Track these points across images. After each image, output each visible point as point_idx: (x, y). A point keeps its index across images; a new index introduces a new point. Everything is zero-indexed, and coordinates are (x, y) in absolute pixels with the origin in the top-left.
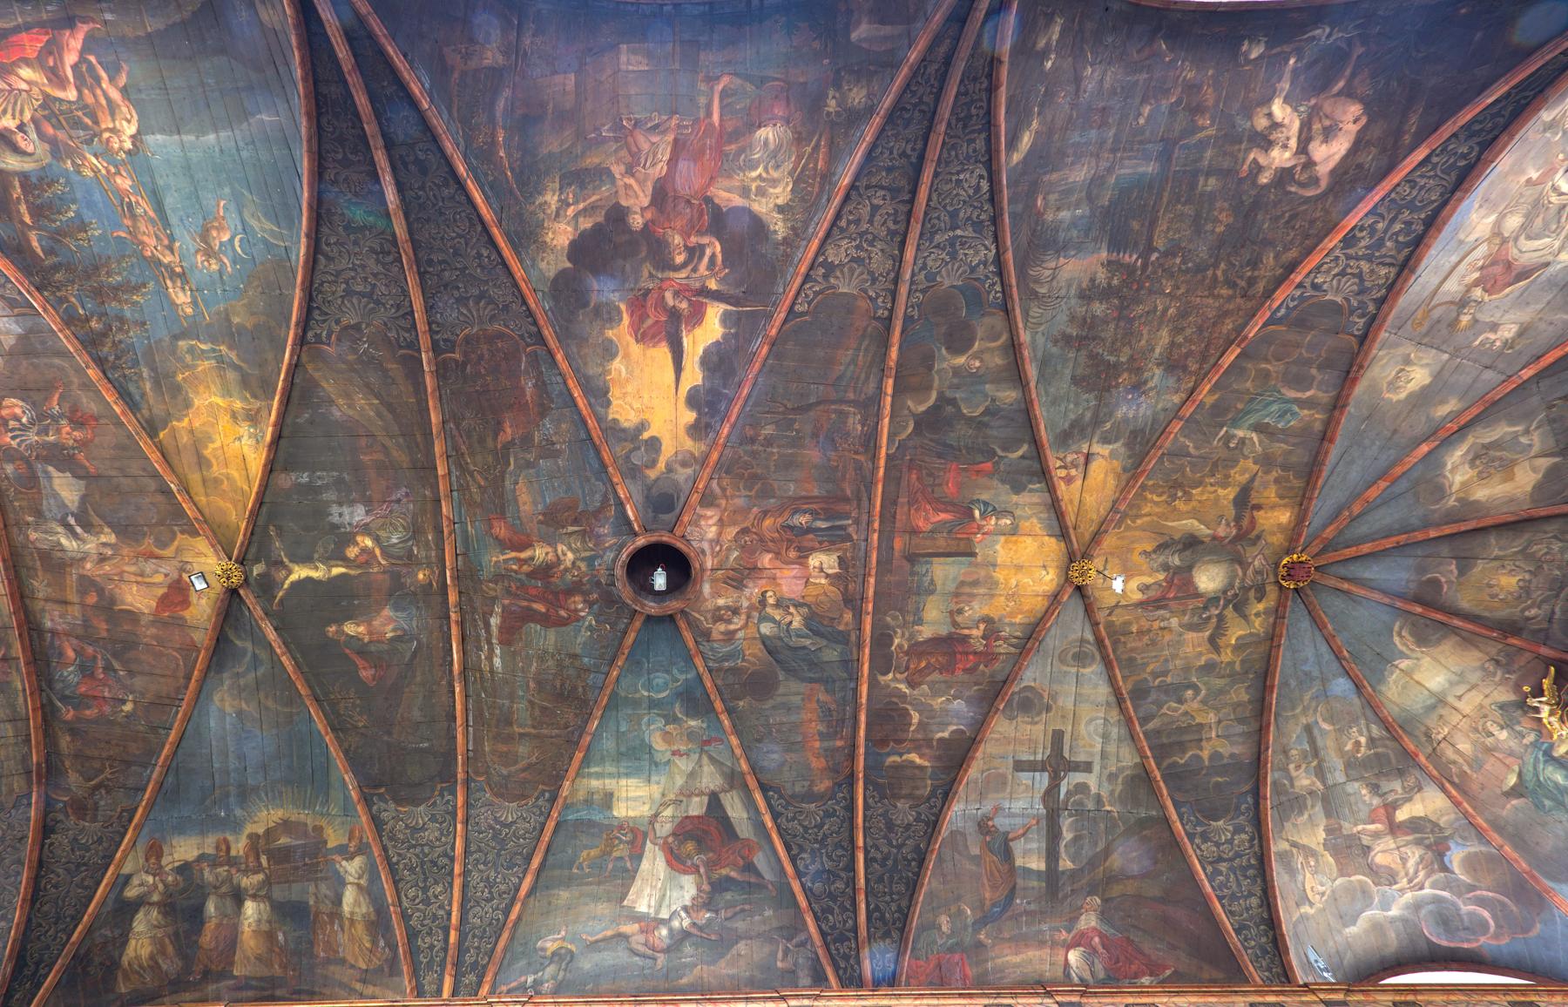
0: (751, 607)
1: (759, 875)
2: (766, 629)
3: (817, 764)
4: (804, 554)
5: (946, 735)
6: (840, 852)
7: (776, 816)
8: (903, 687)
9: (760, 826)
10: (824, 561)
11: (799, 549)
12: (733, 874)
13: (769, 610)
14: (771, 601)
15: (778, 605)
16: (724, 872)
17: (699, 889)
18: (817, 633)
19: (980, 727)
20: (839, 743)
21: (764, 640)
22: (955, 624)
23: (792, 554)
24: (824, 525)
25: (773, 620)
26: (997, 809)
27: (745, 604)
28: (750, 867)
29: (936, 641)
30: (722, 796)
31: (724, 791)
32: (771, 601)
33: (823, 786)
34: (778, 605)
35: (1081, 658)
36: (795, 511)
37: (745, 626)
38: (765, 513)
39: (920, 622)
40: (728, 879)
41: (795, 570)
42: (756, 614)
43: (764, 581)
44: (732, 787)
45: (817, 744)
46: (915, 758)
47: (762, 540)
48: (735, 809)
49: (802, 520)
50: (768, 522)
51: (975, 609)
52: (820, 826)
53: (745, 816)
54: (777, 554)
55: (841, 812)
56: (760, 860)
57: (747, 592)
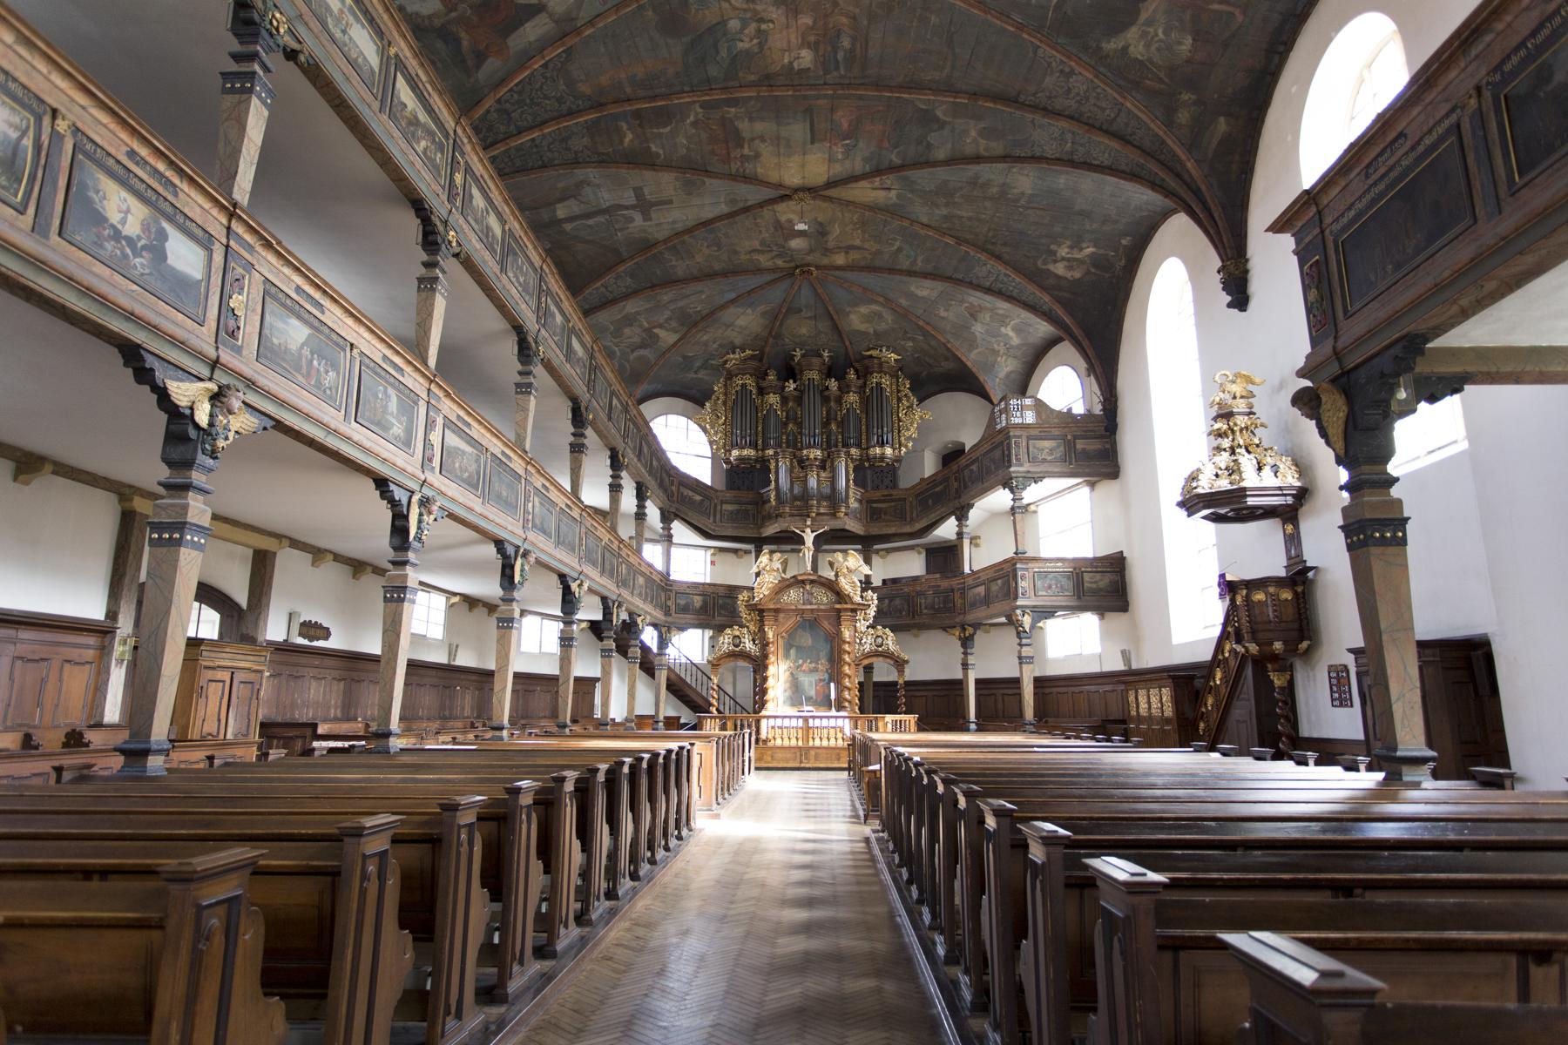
0: (756, 12)
1: (478, 67)
2: (734, 24)
3: (604, 80)
4: (814, 46)
5: (654, 149)
6: (530, 118)
7: (545, 66)
8: (692, 118)
9: (527, 57)
10: (806, 58)
11: (817, 43)
12: (465, 43)
13: (754, 25)
14: (764, 27)
15: (759, 31)
16: (463, 35)
17: (430, 17)
18: (734, 59)
19: (668, 166)
20: (628, 90)
21: (723, 23)
22: (753, 140)
23: (812, 39)
24: (840, 56)
25: (744, 27)
26: (598, 186)
27: (759, 8)
28: (481, 57)
29: (737, 132)
30: (544, 15)
31: (551, 16)
32: (764, 27)
33: (585, 89)
34: (759, 31)
35: (733, 201)
36: (854, 39)
37: (735, 8)
38: (854, 18)
39: (751, 119)
40: (458, 41)
41: (794, 38)
42: (748, 15)
43: (783, 19)
44: (556, 22)
45: (623, 76)
46: (629, 136)
47: (826, 16)
48: (533, 31)
49: (846, 42)
50: (844, 20)
51: (765, 149)
52: (546, 97)
53: (532, 39)
54: (812, 28)
55: (564, 108)
56: (492, 65)
57: (772, 9)
